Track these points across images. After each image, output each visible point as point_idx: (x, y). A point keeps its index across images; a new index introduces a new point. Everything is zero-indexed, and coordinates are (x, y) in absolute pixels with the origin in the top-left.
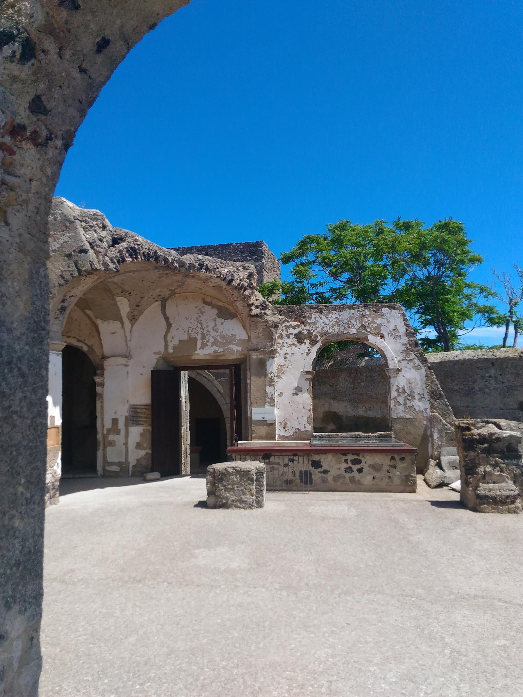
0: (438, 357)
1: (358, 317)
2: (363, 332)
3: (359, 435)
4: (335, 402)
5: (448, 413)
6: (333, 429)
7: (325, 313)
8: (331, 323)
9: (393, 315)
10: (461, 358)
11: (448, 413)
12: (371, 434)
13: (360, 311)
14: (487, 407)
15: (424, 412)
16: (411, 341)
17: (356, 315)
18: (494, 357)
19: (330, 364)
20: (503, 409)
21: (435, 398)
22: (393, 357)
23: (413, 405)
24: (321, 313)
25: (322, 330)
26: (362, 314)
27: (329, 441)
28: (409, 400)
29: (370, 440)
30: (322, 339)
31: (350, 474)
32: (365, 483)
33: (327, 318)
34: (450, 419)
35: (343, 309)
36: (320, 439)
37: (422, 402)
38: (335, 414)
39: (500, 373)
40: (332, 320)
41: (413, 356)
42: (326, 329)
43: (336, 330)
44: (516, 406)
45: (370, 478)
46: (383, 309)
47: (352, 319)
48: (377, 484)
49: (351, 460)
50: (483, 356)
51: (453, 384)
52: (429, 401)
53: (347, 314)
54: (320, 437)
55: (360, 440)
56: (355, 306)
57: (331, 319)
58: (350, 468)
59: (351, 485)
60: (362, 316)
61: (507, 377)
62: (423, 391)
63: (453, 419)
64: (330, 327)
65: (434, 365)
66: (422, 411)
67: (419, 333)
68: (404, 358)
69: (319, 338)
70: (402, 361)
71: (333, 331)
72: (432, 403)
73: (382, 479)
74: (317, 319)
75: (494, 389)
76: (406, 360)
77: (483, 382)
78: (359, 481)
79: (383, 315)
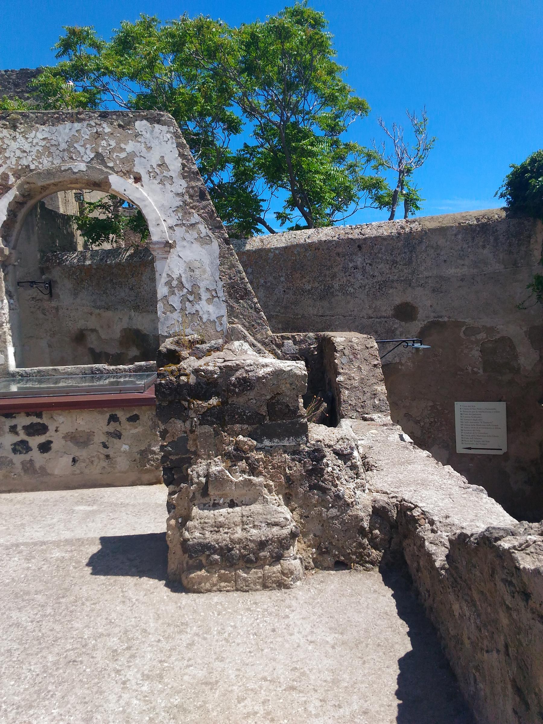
0: (283, 238)
1: (87, 137)
2: (99, 169)
3: (99, 370)
4: (137, 314)
5: (258, 324)
6: (136, 356)
7: (21, 128)
8: (34, 150)
9: (158, 135)
10: (315, 239)
11: (258, 324)
12: (121, 367)
13: (91, 126)
14: (351, 315)
15: (218, 323)
16: (193, 187)
17: (85, 133)
18: (361, 237)
19: (128, 254)
20: (372, 318)
21: (236, 298)
22: (159, 219)
23: (197, 311)
24: (15, 128)
25: (17, 164)
26: (97, 132)
27: (40, 382)
28: (190, 301)
29: (120, 377)
30: (19, 182)
31: (22, 455)
32: (56, 472)
33: (27, 138)
34: (262, 334)
35: (58, 122)
36: (22, 380)
37: (214, 305)
38: (137, 332)
39: (369, 262)
40: (37, 143)
41: (195, 218)
42: (25, 162)
43: (46, 163)
44: (390, 313)
45: (67, 460)
46: (137, 123)
47: (77, 142)
48: (82, 473)
49: (24, 428)
50: (347, 236)
51: (304, 280)
52: (226, 302)
53: (67, 130)
54: (22, 375)
55: (99, 379)
56: (81, 116)
57: (34, 142)
58: (24, 443)
59: (26, 478)
60: (96, 136)
61: (379, 267)
62: (215, 283)
63: (266, 334)
64: (34, 157)
65: (277, 252)
66: (214, 322)
67: (289, 219)
68: (180, 222)
69: (12, 180)
70: (175, 228)
71: (40, 166)
72: (232, 307)
73: (92, 462)
74: (6, 141)
75: (360, 287)
76: (184, 224)
77: (346, 276)
78: (43, 468)
79: (137, 135)
